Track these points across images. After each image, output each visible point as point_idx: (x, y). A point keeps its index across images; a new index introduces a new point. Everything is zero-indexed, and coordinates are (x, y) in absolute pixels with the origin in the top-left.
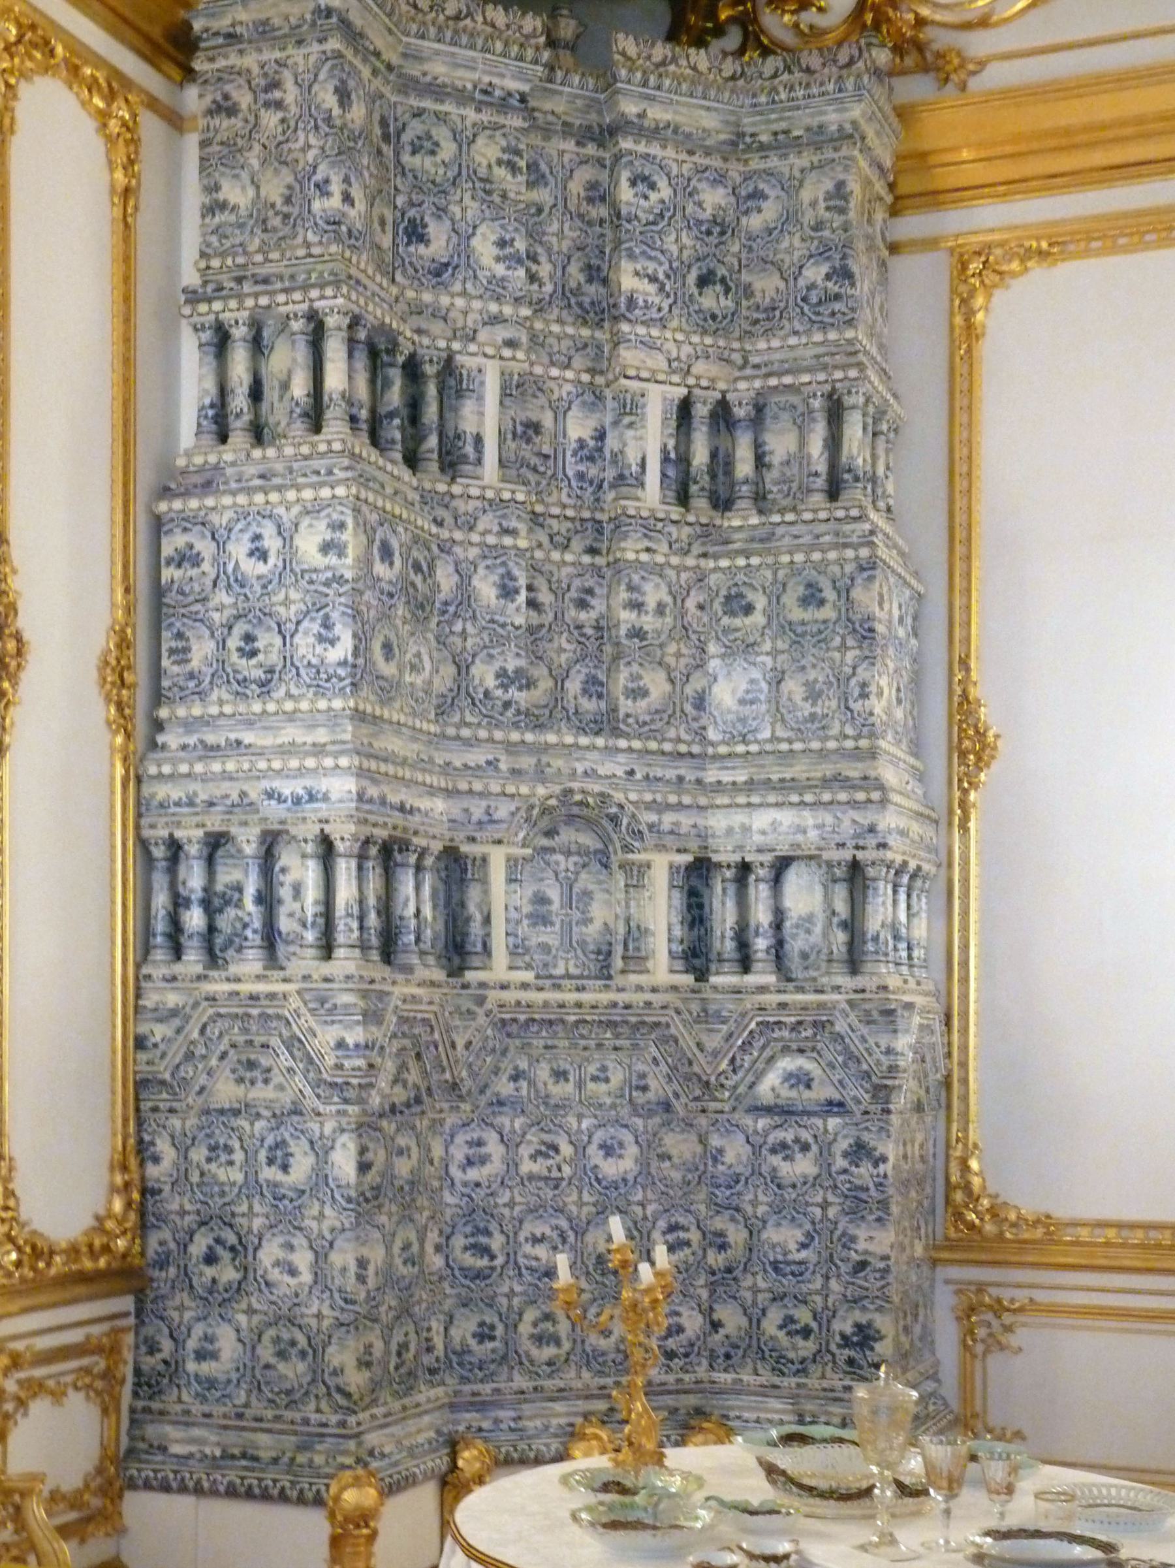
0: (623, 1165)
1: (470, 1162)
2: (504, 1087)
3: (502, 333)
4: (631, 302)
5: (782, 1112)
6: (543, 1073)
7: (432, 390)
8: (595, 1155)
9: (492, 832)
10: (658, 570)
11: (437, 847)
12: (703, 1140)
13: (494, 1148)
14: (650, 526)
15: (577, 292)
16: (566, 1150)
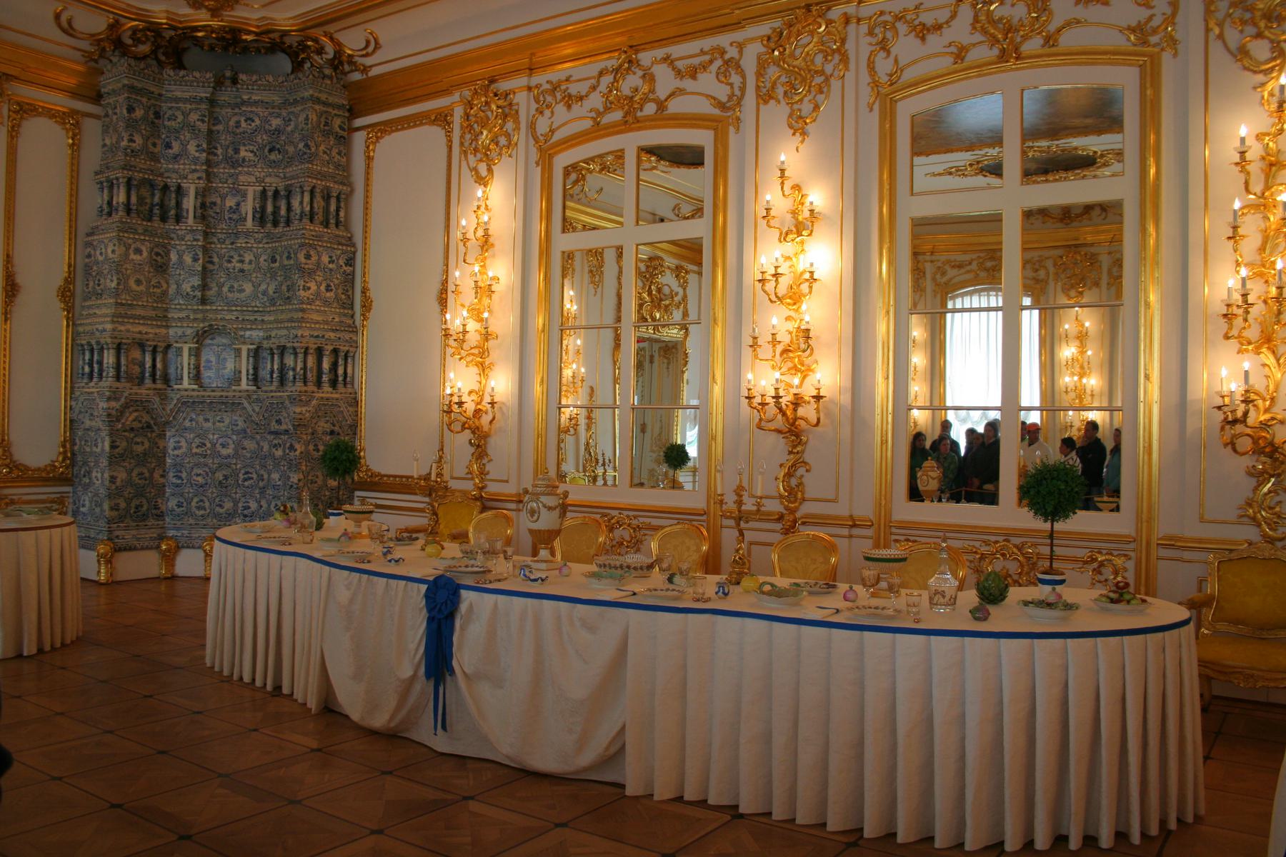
0: (229, 451)
1: (175, 448)
2: (187, 424)
3: (196, 175)
4: (244, 160)
5: (276, 433)
6: (201, 419)
7: (173, 195)
8: (219, 447)
9: (184, 339)
10: (250, 249)
11: (164, 345)
12: (258, 443)
13: (183, 444)
14: (247, 234)
15: (231, 157)
16: (209, 445)
